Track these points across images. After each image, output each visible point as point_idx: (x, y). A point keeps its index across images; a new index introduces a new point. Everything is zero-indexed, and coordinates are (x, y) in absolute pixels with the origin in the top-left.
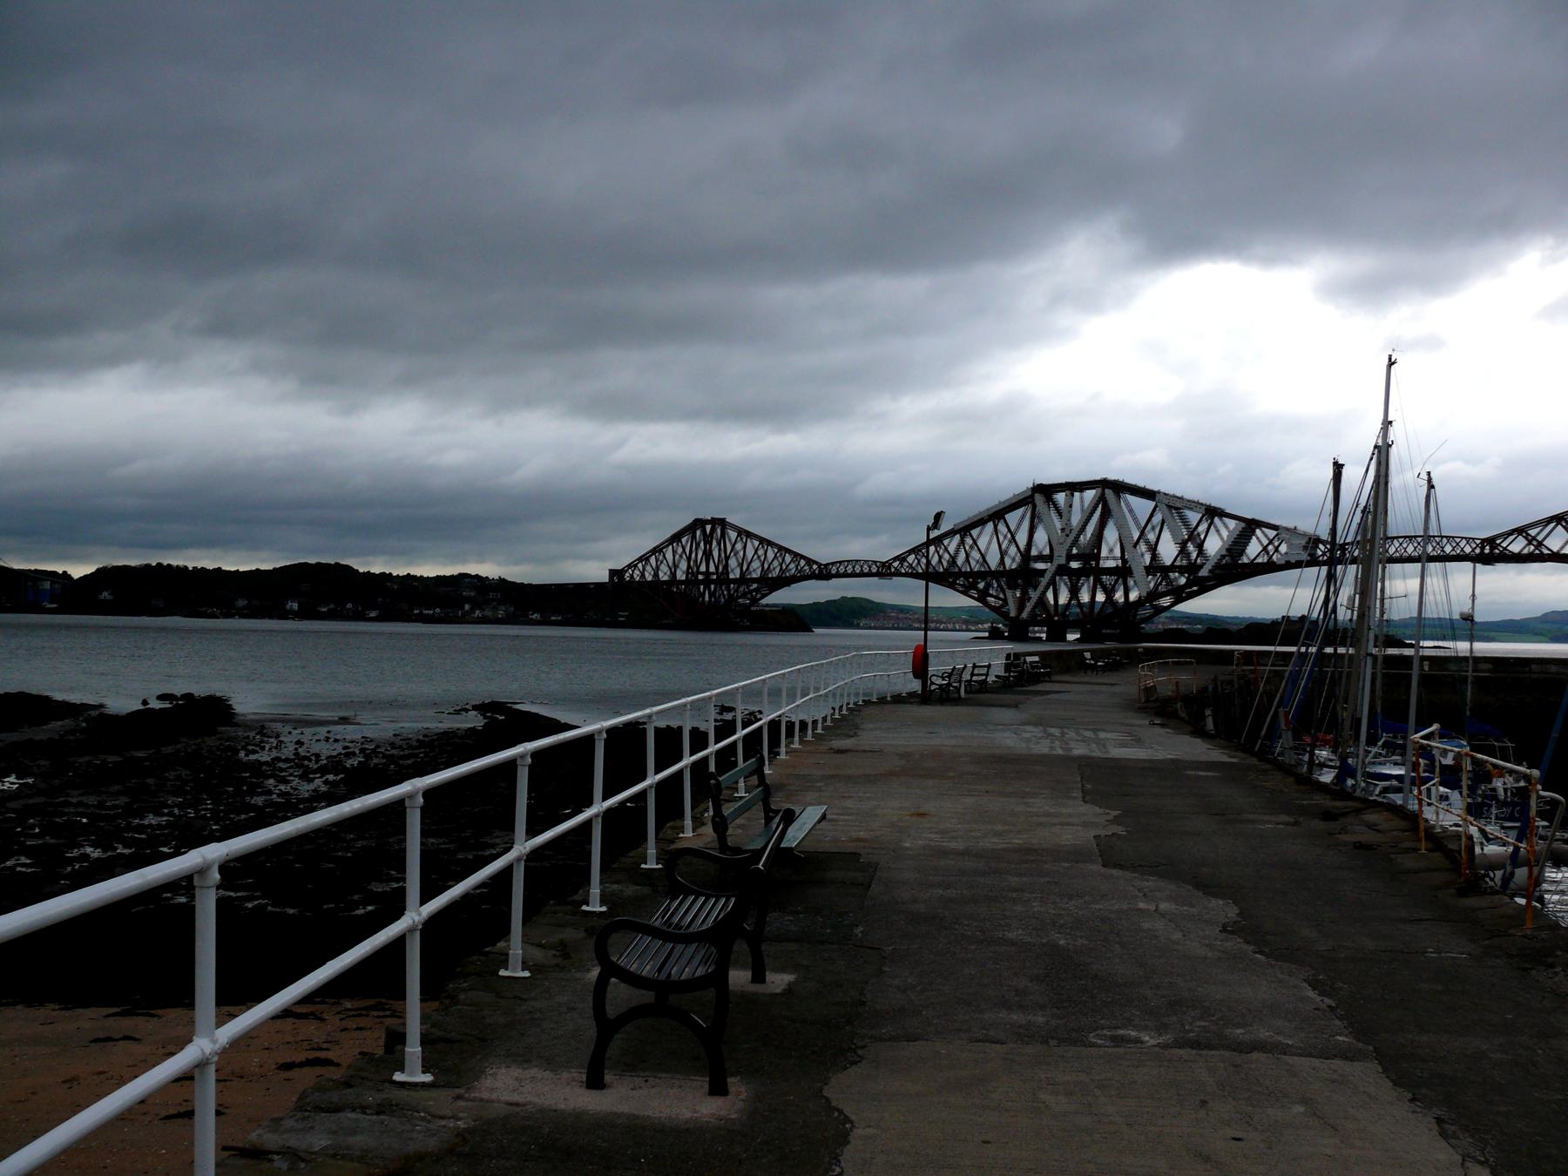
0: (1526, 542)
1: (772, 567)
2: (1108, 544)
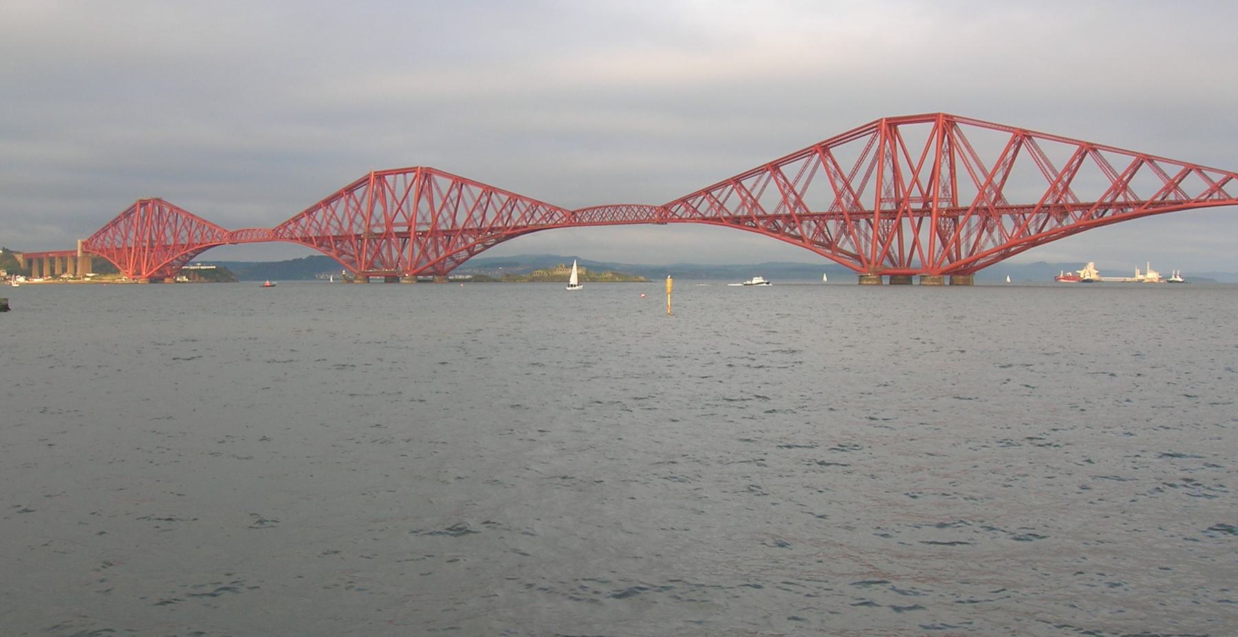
0: (684, 209)
1: (195, 236)
2: (421, 213)
